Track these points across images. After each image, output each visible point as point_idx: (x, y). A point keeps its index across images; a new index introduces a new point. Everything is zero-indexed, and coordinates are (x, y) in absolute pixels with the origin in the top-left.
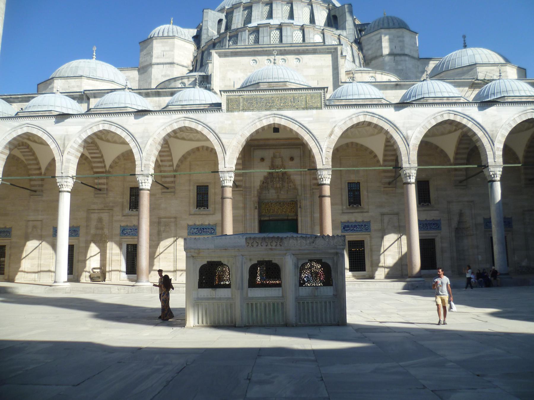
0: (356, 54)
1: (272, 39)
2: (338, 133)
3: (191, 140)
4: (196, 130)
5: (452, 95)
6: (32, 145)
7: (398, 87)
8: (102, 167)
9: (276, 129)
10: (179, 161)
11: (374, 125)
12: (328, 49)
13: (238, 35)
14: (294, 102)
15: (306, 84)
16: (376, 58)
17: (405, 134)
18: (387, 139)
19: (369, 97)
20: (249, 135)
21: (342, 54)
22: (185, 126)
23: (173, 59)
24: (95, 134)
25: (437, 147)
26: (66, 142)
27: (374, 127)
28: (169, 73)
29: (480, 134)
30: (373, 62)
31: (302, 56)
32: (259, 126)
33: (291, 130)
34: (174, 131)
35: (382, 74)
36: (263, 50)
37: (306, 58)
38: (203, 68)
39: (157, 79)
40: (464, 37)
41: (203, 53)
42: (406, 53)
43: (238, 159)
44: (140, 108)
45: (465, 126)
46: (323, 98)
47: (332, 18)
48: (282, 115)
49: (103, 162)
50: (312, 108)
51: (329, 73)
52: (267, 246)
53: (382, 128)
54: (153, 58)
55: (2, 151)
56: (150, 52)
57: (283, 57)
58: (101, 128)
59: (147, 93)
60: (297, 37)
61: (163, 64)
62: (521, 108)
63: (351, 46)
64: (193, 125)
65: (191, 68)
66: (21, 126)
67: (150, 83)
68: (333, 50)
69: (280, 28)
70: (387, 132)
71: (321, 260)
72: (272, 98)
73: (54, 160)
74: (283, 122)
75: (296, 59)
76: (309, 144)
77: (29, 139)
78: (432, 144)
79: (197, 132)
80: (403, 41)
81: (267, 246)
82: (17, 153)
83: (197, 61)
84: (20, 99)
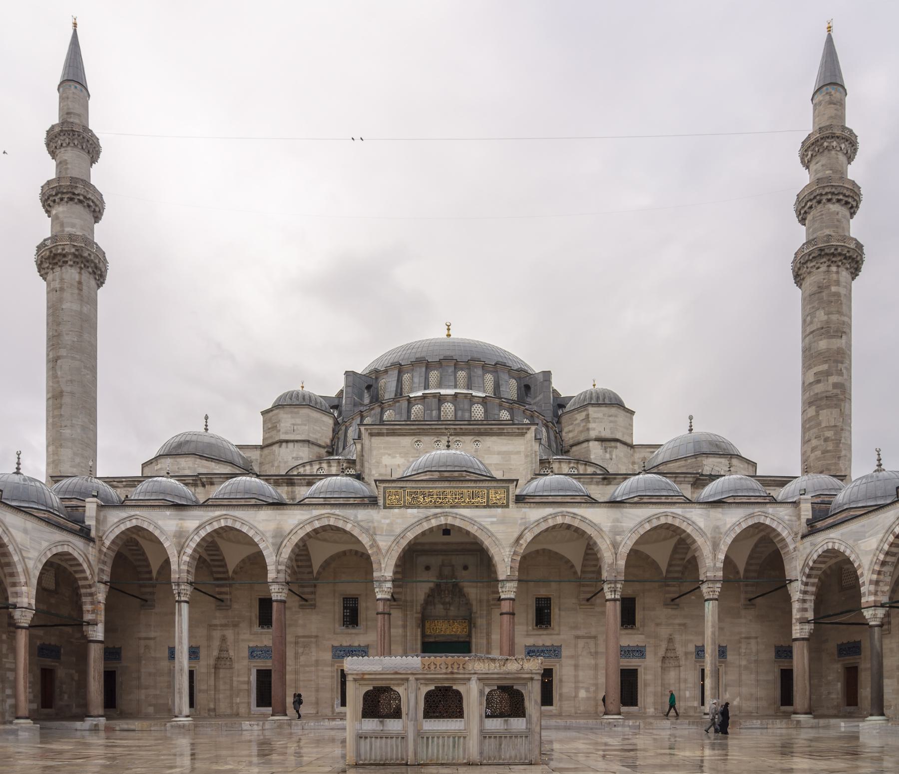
2: (529, 537)
4: (344, 529)
11: (574, 528)
12: (518, 429)
14: (473, 499)
22: (329, 525)
27: (574, 531)
31: (484, 437)
32: (426, 526)
33: (468, 533)
34: (316, 531)
36: (432, 429)
46: (510, 493)
48: (457, 514)
50: (495, 506)
53: (584, 532)
54: (281, 433)
56: (275, 425)
57: (458, 438)
60: (478, 411)
64: (340, 524)
72: (444, 491)
74: (457, 523)
79: (345, 531)
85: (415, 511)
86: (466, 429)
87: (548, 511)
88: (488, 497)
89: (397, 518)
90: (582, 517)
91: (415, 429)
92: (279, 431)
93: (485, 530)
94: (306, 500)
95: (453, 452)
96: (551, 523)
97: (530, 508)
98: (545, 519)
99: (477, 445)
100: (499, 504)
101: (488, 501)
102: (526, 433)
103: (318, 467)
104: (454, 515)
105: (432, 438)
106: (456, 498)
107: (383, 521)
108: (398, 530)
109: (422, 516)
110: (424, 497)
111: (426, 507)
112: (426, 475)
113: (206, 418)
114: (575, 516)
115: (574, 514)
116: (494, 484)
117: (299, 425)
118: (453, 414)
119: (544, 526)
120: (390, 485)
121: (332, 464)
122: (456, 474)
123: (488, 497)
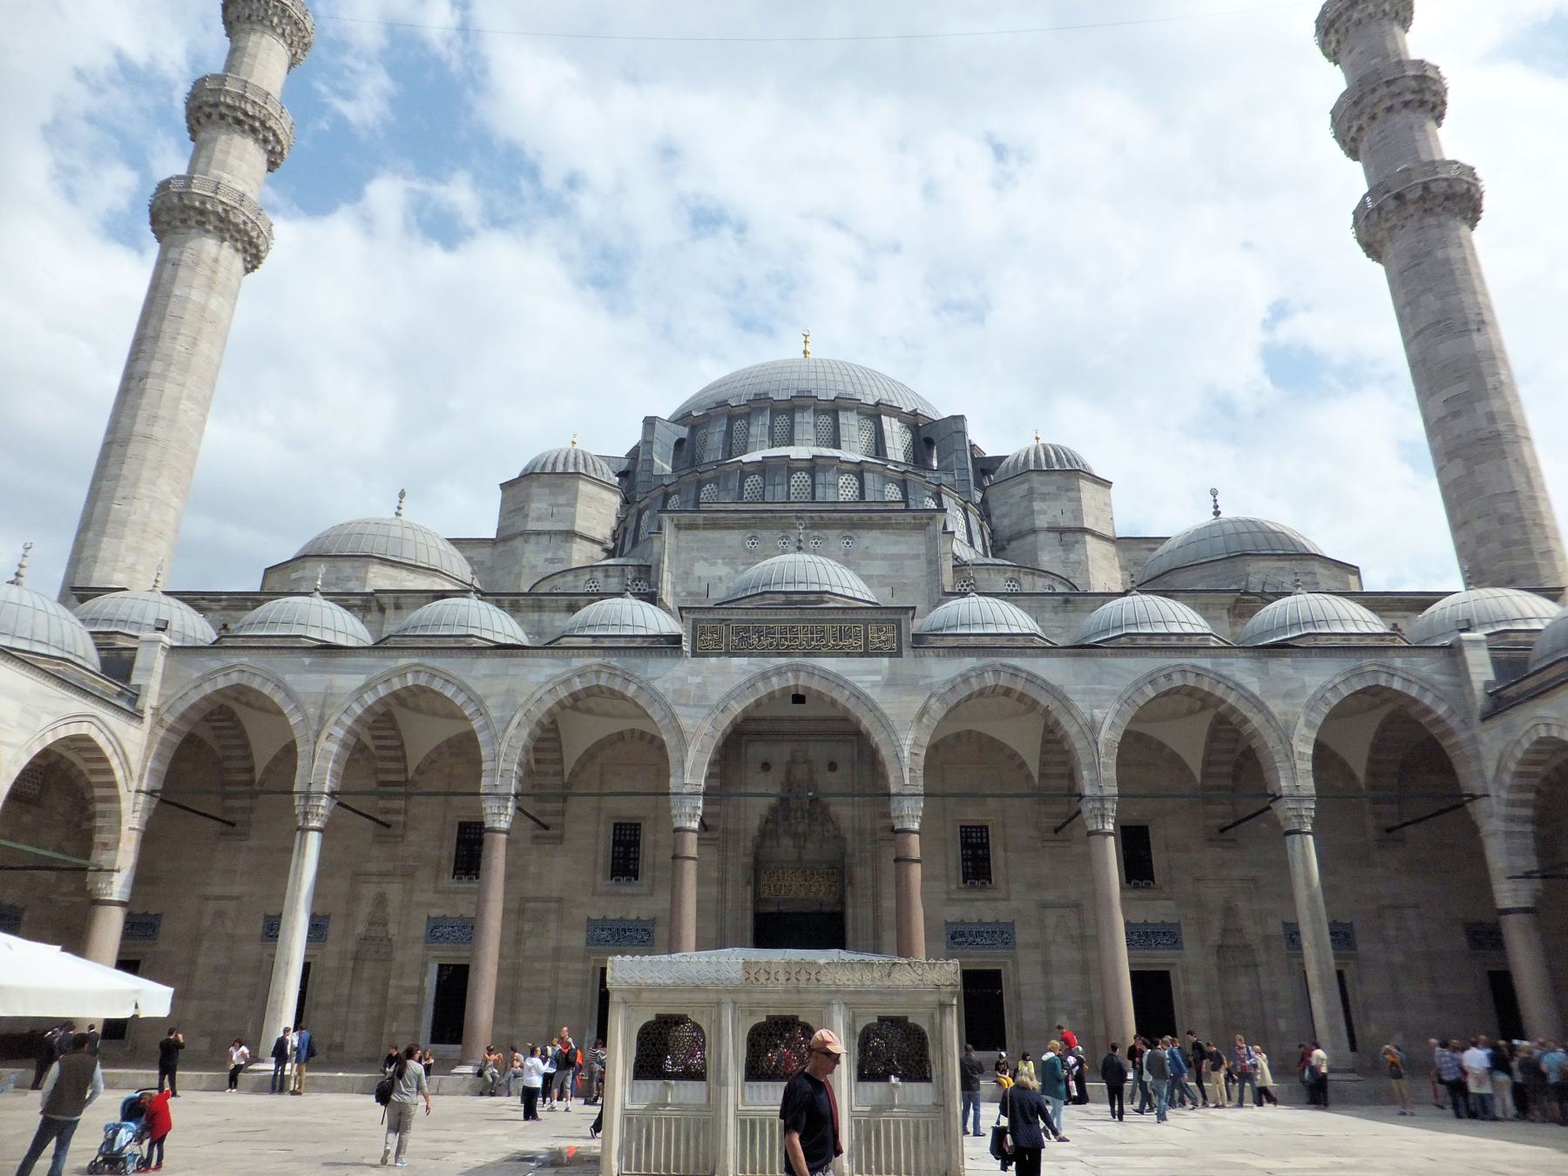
0: (975, 527)
1: (792, 490)
2: (938, 710)
3: (607, 715)
5: (1188, 629)
6: (241, 711)
7: (1070, 608)
8: (398, 771)
9: (799, 699)
10: (578, 761)
11: (1016, 696)
12: (914, 518)
13: (718, 477)
15: (867, 598)
16: (1020, 535)
17: (1088, 716)
18: (1046, 725)
19: (1005, 630)
20: (740, 710)
21: (945, 527)
23: (573, 522)
24: (395, 695)
25: (1161, 747)
26: (328, 712)
28: (561, 554)
29: (1256, 720)
30: (1014, 544)
32: (763, 690)
33: (833, 702)
34: (574, 696)
35: (1033, 574)
36: (775, 517)
37: (868, 539)
38: (639, 548)
39: (534, 567)
40: (1214, 493)
41: (640, 513)
42: (1086, 526)
43: (712, 764)
44: (502, 640)
45: (1222, 701)
47: (923, 444)
48: (814, 667)
49: (404, 757)
50: (879, 653)
51: (915, 571)
52: (788, 980)
53: (1035, 703)
54: (529, 519)
55: (174, 727)
58: (410, 680)
59: (511, 602)
61: (549, 533)
62: (1350, 663)
63: (965, 510)
64: (617, 685)
65: (611, 545)
66: (226, 671)
67: (519, 575)
68: (925, 521)
69: (813, 466)
70: (1047, 712)
71: (906, 1018)
72: (793, 627)
73: (290, 751)
74: (816, 684)
75: (845, 538)
76: (873, 735)
77: (237, 700)
78: (1150, 738)
79: (624, 697)
80: (1079, 500)
81: (788, 980)
82: (206, 734)
83: (625, 529)
84: (224, 603)
85: (744, 661)
86: (830, 519)
87: (969, 662)
88: (866, 638)
89: (714, 674)
90: (1029, 673)
91: (749, 519)
92: (526, 516)
93: (862, 698)
94: (562, 640)
95: (807, 557)
96: (976, 685)
97: (938, 656)
98: (965, 679)
99: (848, 543)
100: (885, 650)
101: (866, 645)
102: (928, 524)
103: (588, 577)
104: (810, 670)
105: (776, 532)
106: (812, 639)
107: (690, 679)
108: (715, 695)
109: (756, 670)
110: (759, 638)
111: (763, 655)
112: (763, 599)
113: (402, 494)
114: (1016, 673)
115: (1016, 668)
116: (877, 615)
117: (562, 505)
118: (809, 490)
119: (964, 692)
120: (704, 617)
121: (611, 573)
122: (812, 598)
123: (866, 638)
